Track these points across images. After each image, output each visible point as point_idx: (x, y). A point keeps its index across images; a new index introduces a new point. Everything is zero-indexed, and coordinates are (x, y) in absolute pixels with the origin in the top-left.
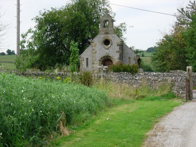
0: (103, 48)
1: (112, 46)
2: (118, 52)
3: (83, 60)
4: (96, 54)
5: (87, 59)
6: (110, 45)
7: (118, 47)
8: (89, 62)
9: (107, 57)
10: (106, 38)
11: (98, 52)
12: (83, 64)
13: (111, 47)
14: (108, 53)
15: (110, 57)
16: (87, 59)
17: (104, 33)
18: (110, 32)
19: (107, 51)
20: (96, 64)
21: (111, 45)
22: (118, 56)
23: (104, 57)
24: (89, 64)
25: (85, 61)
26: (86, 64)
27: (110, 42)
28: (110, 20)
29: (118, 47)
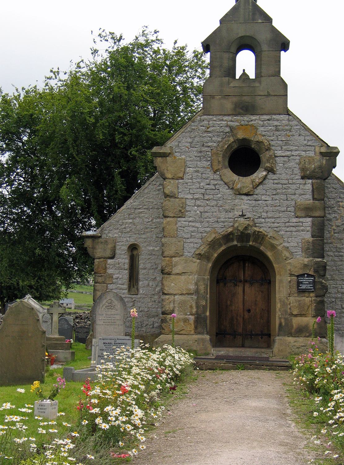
0: (224, 190)
1: (271, 176)
2: (307, 211)
3: (108, 253)
4: (182, 222)
5: (133, 248)
6: (261, 173)
7: (309, 185)
8: (143, 263)
9: (244, 236)
10: (241, 135)
11: (193, 211)
12: (111, 276)
13: (269, 184)
14: (248, 215)
15: (259, 237)
16: (133, 248)
17: (228, 105)
18: (259, 101)
19: (244, 203)
20: (183, 278)
21: (271, 170)
22: (308, 236)
23: (228, 237)
24: (142, 274)
25: (123, 259)
26: (125, 275)
27: (264, 157)
28: (263, 36)
29: (309, 185)
